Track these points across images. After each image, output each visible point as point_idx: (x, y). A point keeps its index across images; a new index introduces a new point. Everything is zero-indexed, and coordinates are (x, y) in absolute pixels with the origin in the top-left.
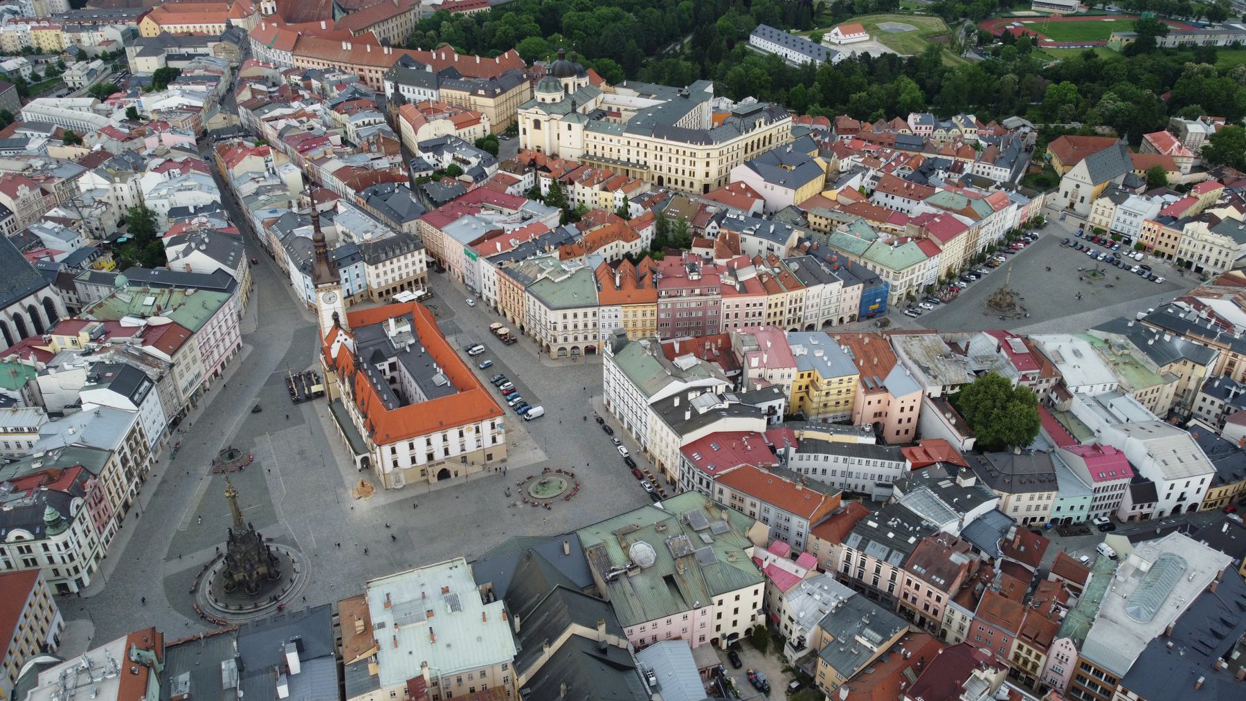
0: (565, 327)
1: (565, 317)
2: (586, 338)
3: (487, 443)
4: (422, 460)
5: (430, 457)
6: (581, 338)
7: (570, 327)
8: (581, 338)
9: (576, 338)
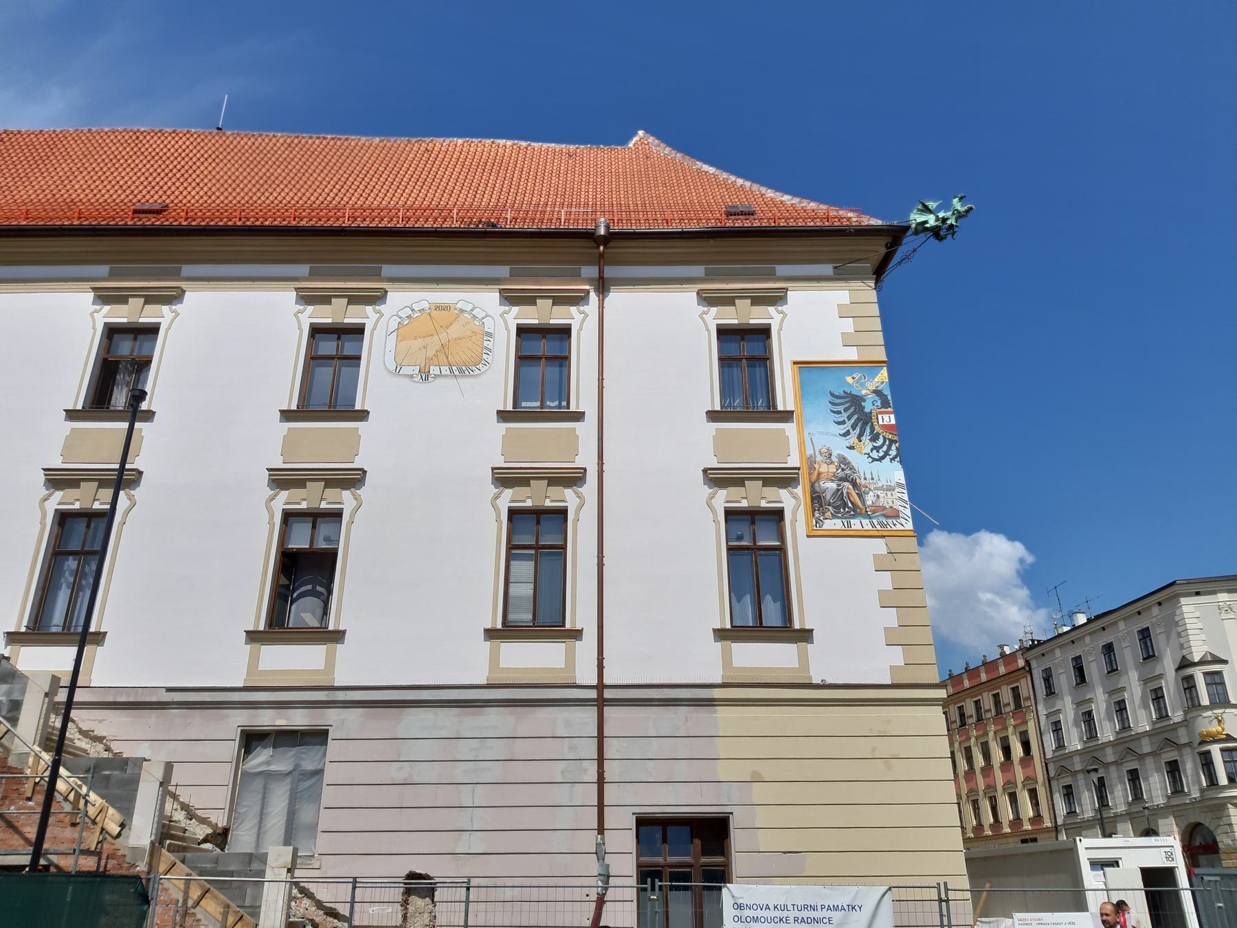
3: (655, 594)
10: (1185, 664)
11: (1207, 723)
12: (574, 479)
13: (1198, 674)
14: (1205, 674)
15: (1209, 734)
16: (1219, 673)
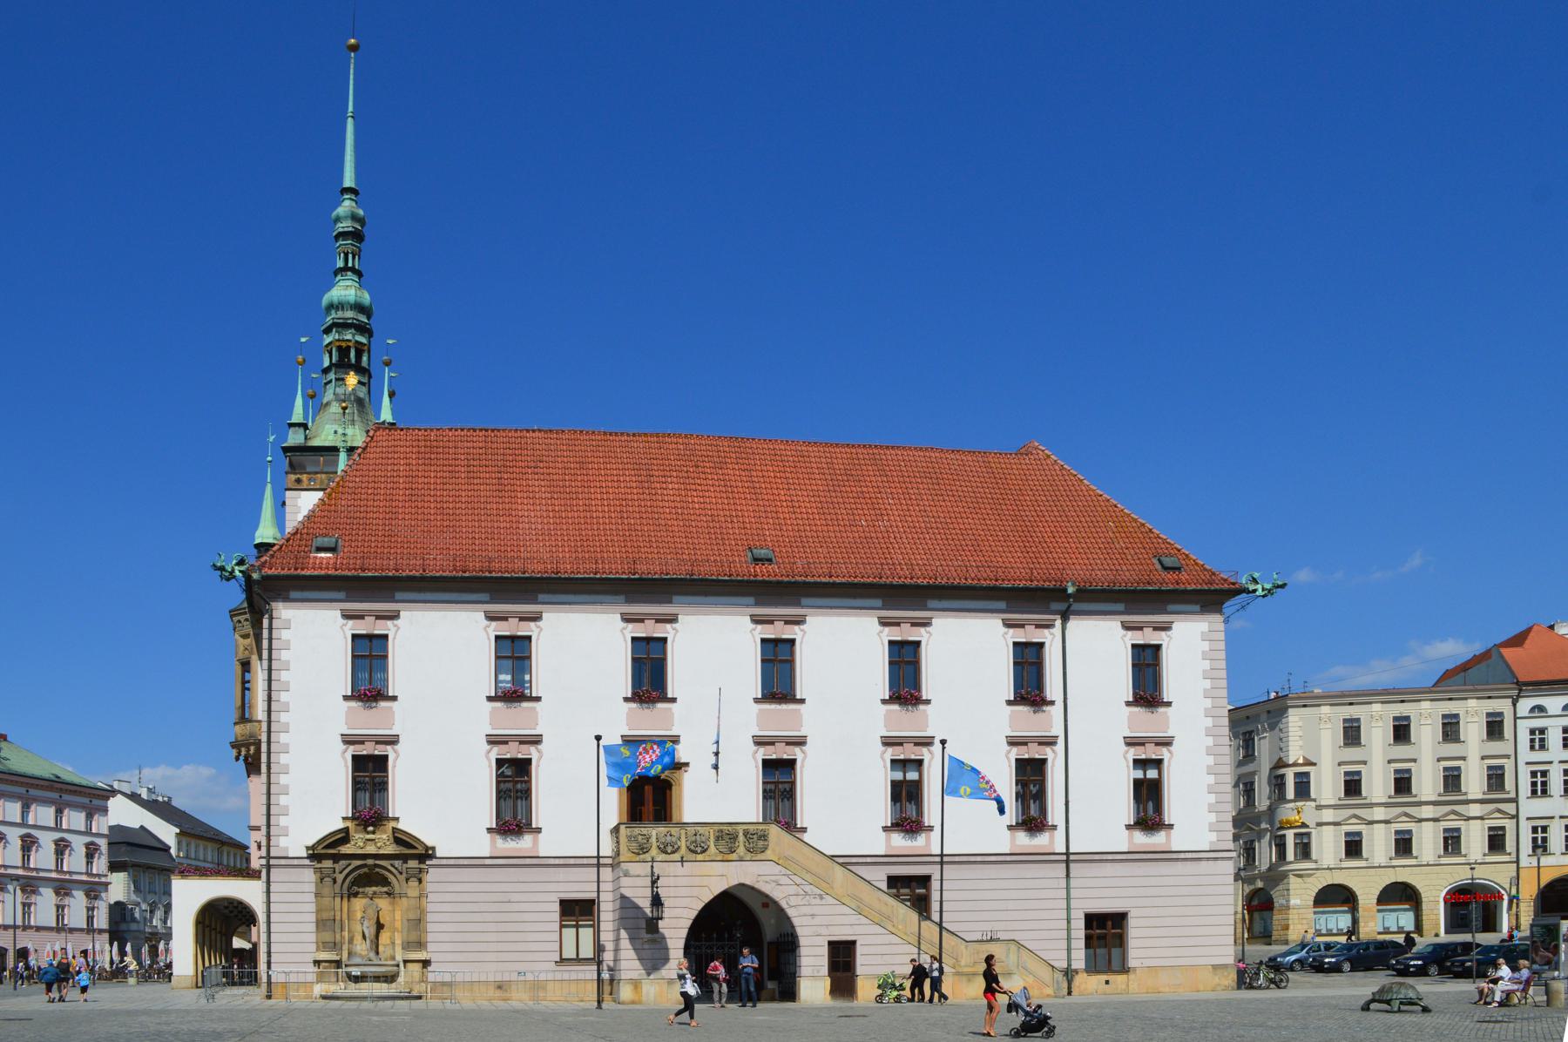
0: (1353, 786)
1: (1352, 734)
2: (1452, 842)
3: (1094, 805)
4: (576, 809)
5: (650, 797)
6: (1427, 841)
7: (1378, 785)
8: (1427, 841)
9: (1404, 845)
10: (1281, 764)
11: (1288, 812)
12: (1050, 742)
13: (1290, 775)
14: (1297, 775)
15: (1288, 822)
16: (1307, 774)
